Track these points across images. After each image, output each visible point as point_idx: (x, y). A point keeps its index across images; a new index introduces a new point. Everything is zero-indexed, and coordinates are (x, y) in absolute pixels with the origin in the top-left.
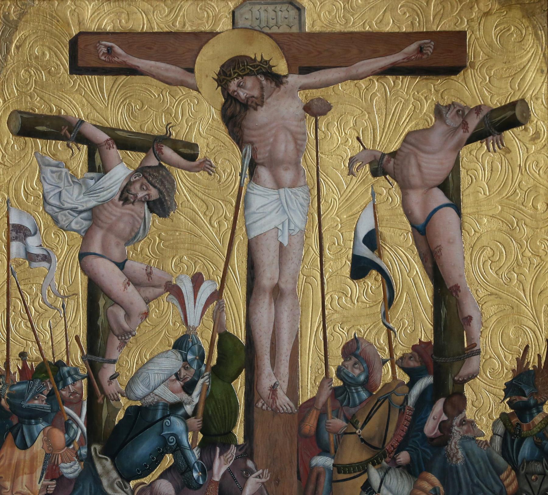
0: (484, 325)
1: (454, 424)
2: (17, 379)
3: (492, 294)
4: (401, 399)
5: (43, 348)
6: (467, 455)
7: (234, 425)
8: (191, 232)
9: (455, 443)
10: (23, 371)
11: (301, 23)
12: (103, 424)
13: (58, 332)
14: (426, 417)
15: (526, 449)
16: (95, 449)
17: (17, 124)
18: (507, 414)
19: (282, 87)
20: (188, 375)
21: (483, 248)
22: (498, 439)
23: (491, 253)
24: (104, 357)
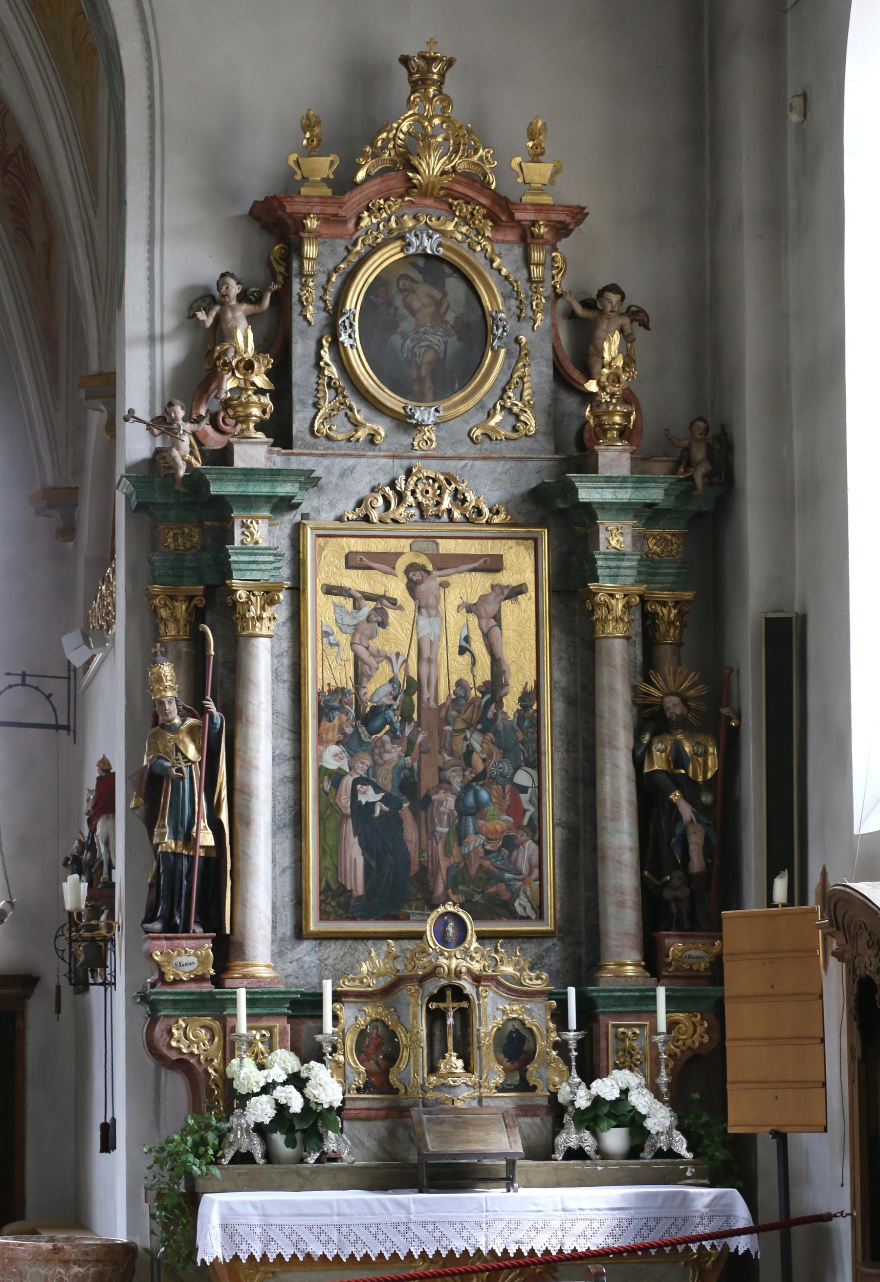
10: (329, 691)
15: (526, 723)
20: (395, 693)
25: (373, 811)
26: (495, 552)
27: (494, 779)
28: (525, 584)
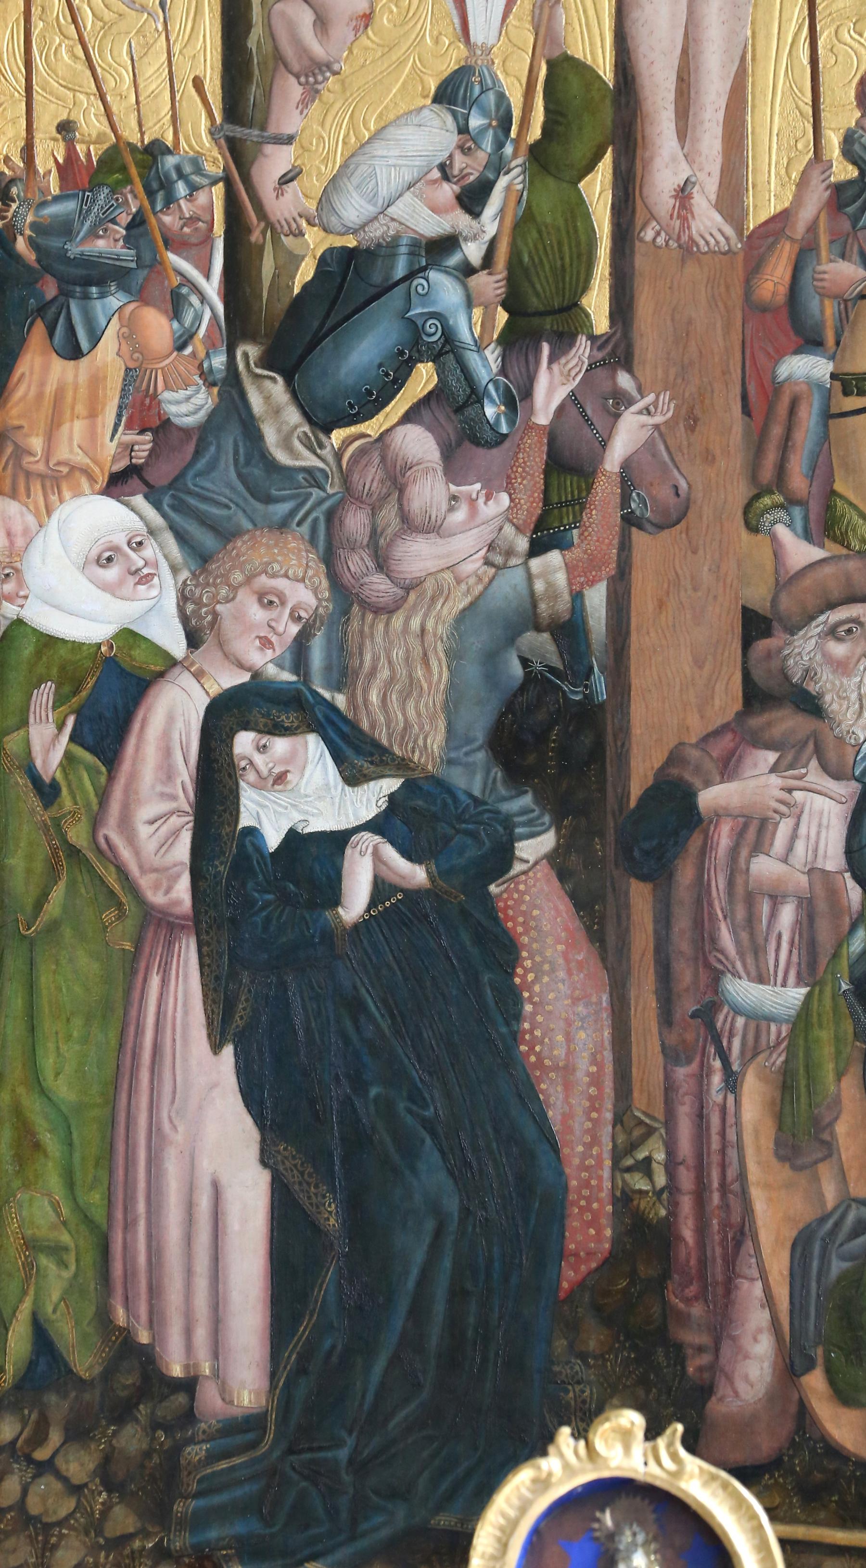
2: (54, 188)
5: (114, 109)
7: (585, 287)
13: (151, 71)
16: (246, 356)
24: (263, 128)
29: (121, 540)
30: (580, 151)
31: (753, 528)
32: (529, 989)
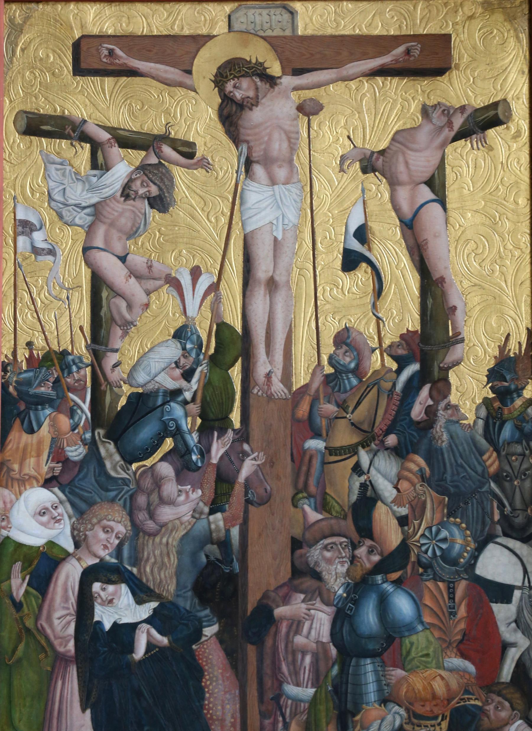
0: (468, 314)
1: (439, 408)
2: (24, 367)
3: (475, 285)
4: (389, 385)
5: (49, 337)
6: (452, 437)
7: (231, 410)
8: (190, 227)
9: (441, 426)
10: (30, 360)
11: (294, 26)
12: (107, 410)
13: (63, 323)
14: (413, 402)
15: (507, 432)
16: (99, 433)
17: (23, 123)
18: (490, 399)
19: (276, 88)
20: (187, 363)
21: (468, 241)
22: (481, 422)
23: (475, 246)
24: (107, 346)
25: (131, 648)
26: (432, 28)
27: (427, 567)
28: (505, 100)
29: (49, 505)
30: (229, 358)
31: (295, 506)
32: (208, 688)
